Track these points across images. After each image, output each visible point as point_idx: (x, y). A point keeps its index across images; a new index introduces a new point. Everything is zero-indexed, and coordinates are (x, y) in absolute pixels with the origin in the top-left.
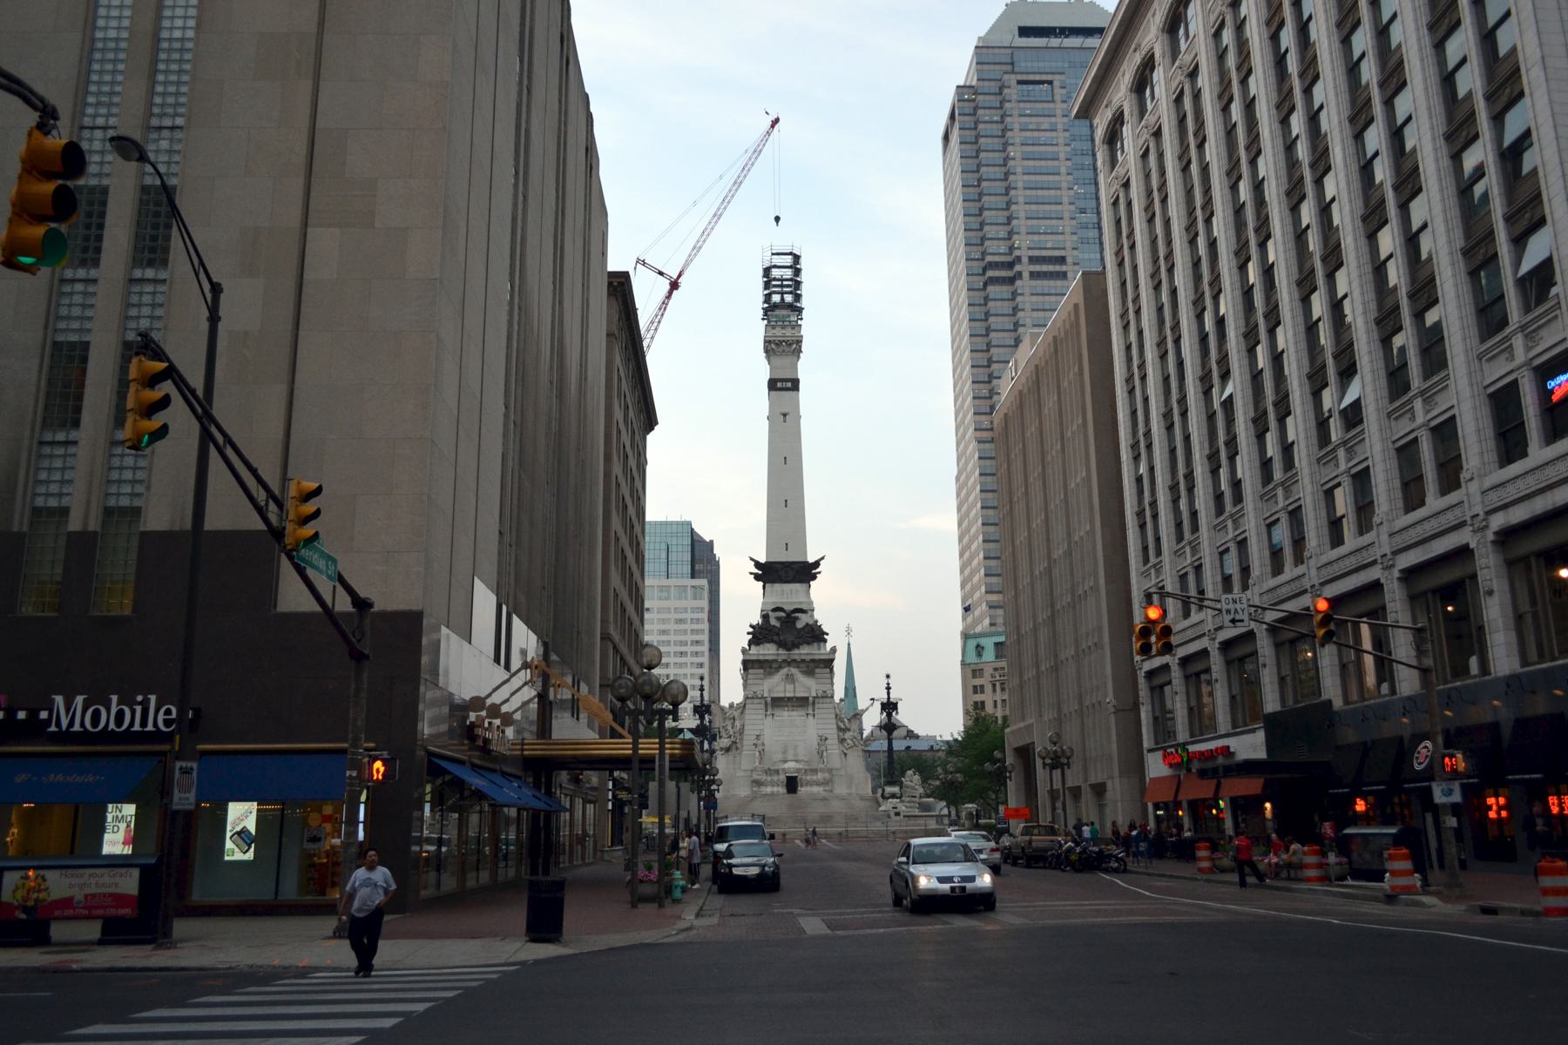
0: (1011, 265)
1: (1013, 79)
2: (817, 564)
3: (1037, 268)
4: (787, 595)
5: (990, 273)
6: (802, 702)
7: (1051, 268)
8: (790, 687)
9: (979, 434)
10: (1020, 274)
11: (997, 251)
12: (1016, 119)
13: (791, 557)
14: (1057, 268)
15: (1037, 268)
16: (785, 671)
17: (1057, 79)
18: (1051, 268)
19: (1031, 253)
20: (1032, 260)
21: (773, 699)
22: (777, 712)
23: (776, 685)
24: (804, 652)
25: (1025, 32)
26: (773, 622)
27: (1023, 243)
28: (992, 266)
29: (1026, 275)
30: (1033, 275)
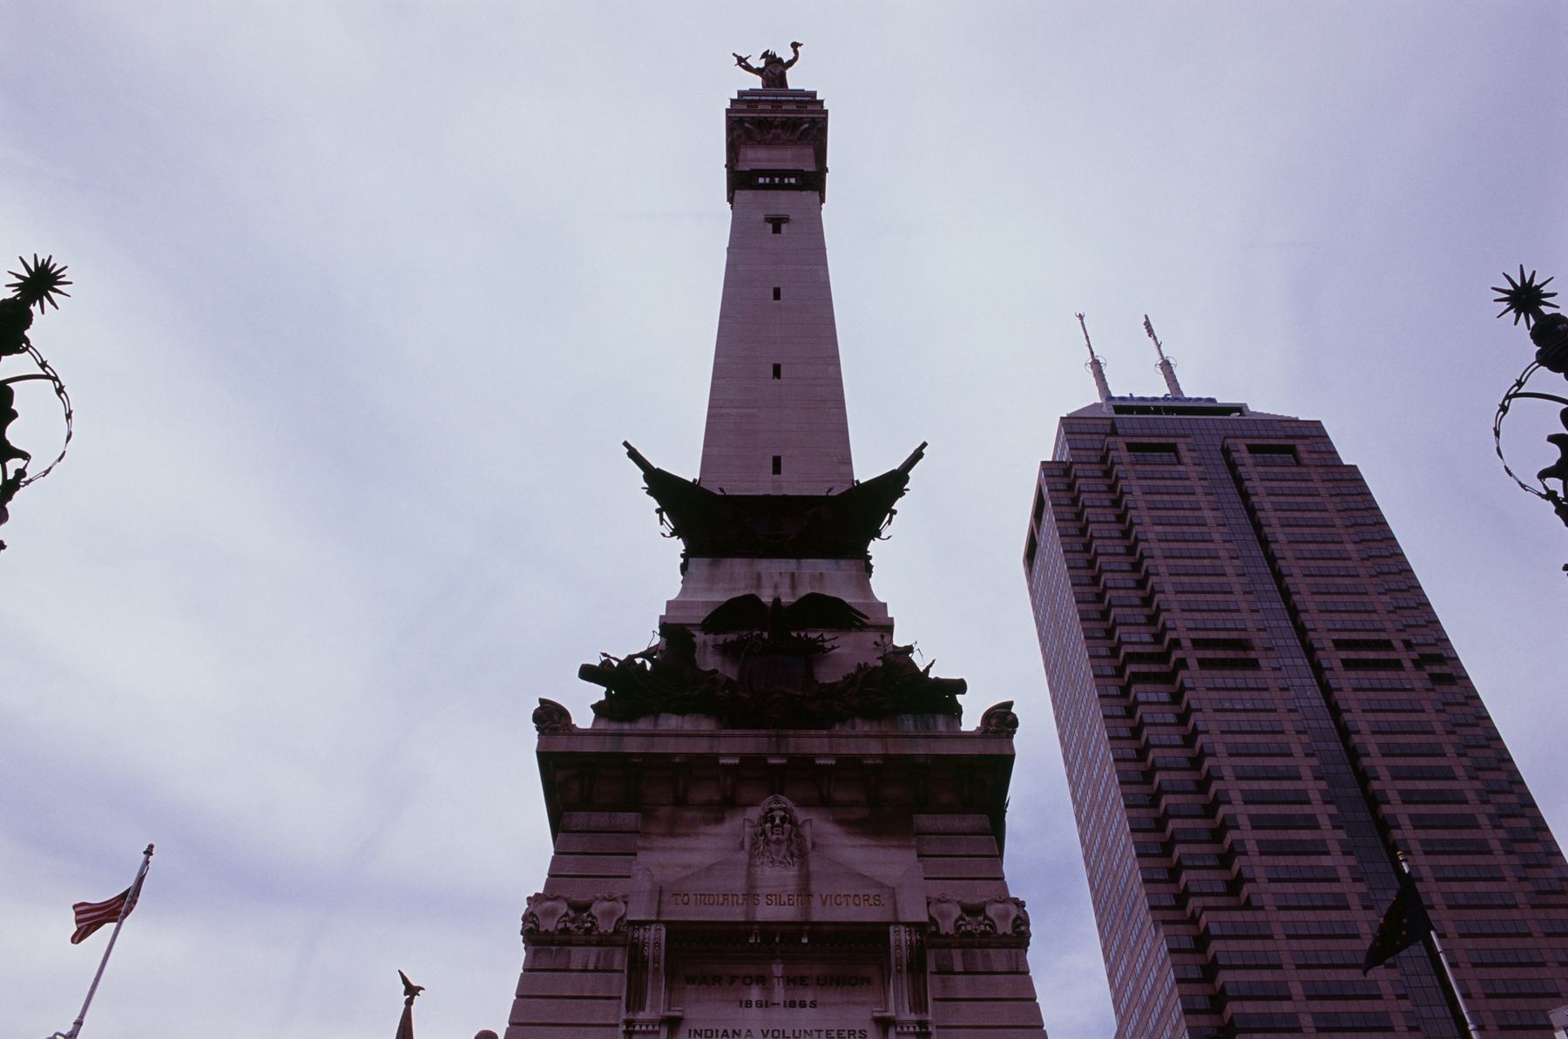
0: (1163, 658)
1: (1120, 442)
2: (893, 485)
3: (1209, 654)
4: (777, 580)
5: (1132, 668)
6: (840, 955)
7: (1231, 654)
8: (777, 876)
9: (1159, 915)
10: (1182, 664)
11: (1136, 637)
12: (1134, 482)
13: (793, 484)
14: (1241, 655)
15: (1209, 654)
16: (754, 813)
17: (1182, 445)
18: (1231, 654)
19: (1194, 635)
20: (1197, 643)
21: (678, 932)
22: (705, 1012)
23: (703, 868)
24: (863, 741)
25: (1118, 409)
26: (709, 661)
27: (1180, 624)
28: (1131, 658)
29: (1192, 662)
30: (1203, 663)
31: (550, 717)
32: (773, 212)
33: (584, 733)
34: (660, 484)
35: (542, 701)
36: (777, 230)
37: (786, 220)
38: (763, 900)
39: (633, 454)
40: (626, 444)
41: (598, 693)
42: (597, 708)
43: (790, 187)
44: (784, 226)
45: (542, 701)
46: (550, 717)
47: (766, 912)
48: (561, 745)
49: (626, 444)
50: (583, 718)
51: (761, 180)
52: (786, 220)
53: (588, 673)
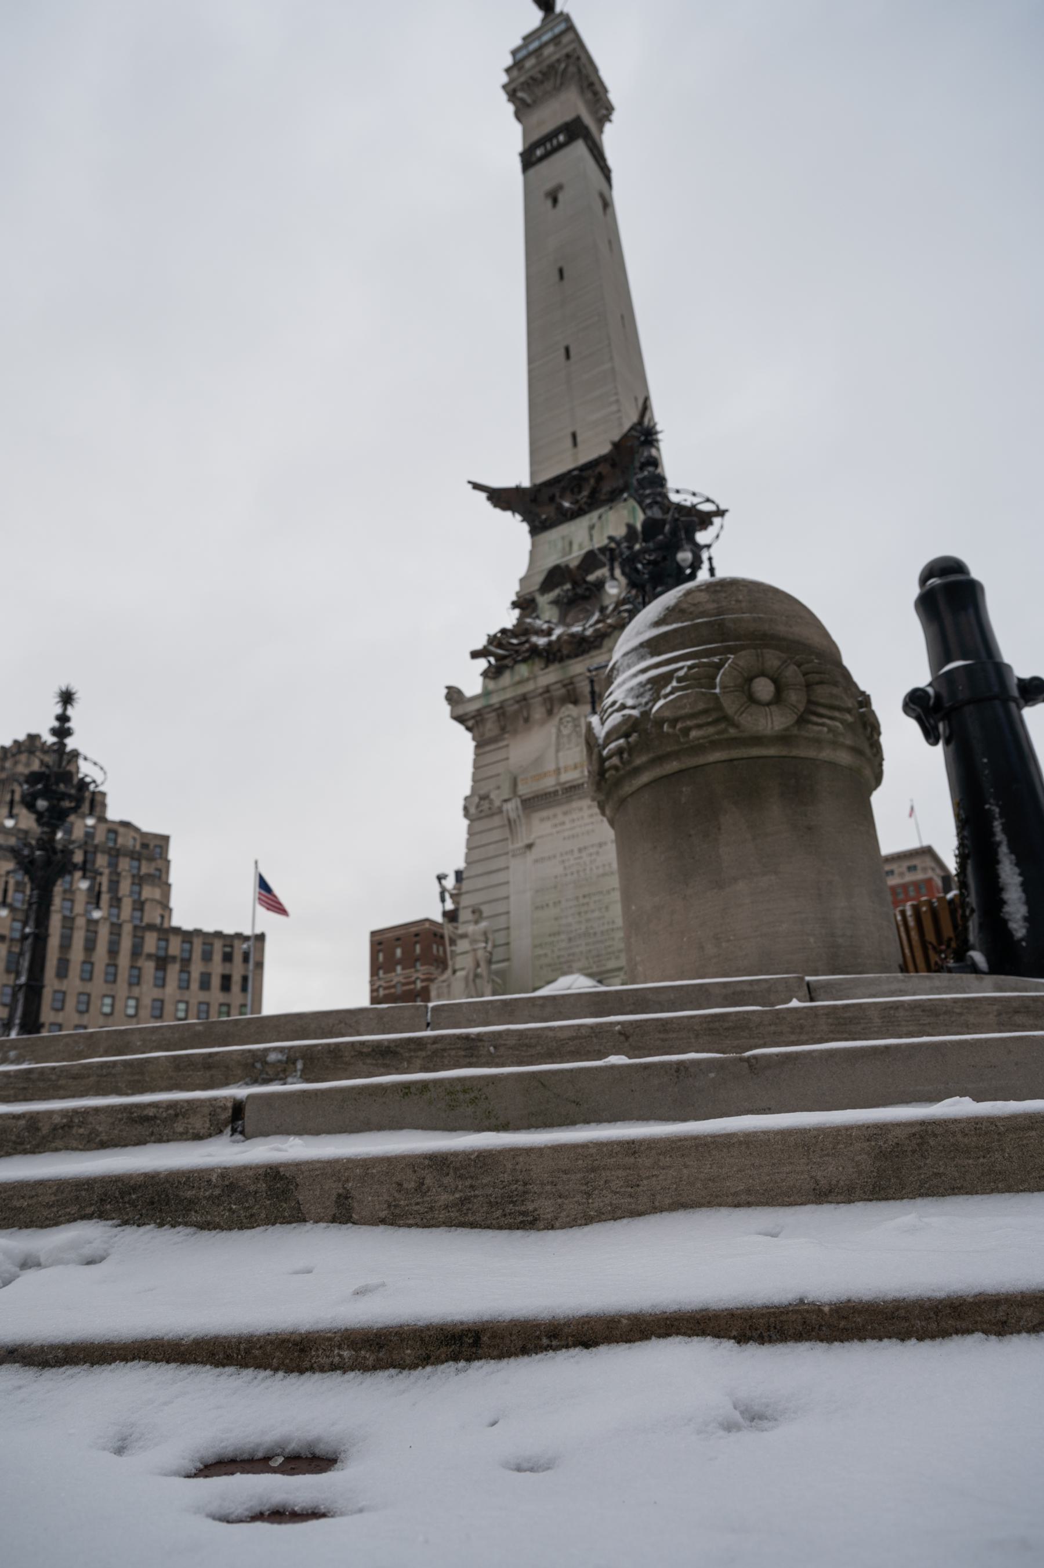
31: (453, 695)
32: (549, 186)
34: (501, 498)
35: (448, 688)
36: (555, 201)
37: (560, 188)
38: (562, 771)
39: (477, 486)
40: (469, 482)
41: (482, 664)
42: (485, 674)
43: (561, 146)
44: (561, 197)
45: (448, 688)
46: (453, 695)
47: (565, 777)
48: (460, 710)
49: (469, 482)
51: (539, 152)
52: (560, 188)
53: (475, 655)
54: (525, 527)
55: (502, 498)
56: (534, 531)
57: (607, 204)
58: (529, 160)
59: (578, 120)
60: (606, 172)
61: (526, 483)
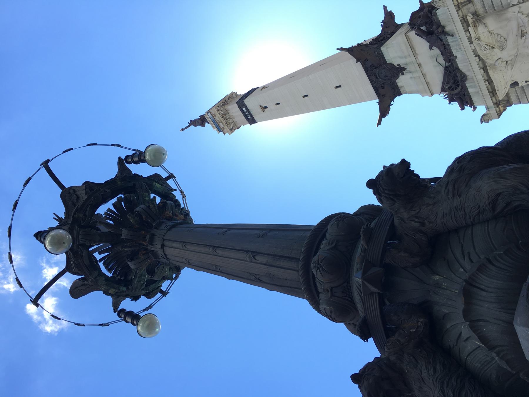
31: (485, 119)
32: (260, 110)
33: (487, 108)
34: (384, 112)
35: (482, 122)
36: (266, 107)
39: (379, 123)
43: (247, 109)
44: (264, 106)
46: (485, 119)
50: (481, 110)
54: (397, 99)
55: (384, 112)
56: (399, 94)
57: (264, 87)
58: (252, 121)
59: (238, 103)
60: (253, 90)
61: (377, 101)
